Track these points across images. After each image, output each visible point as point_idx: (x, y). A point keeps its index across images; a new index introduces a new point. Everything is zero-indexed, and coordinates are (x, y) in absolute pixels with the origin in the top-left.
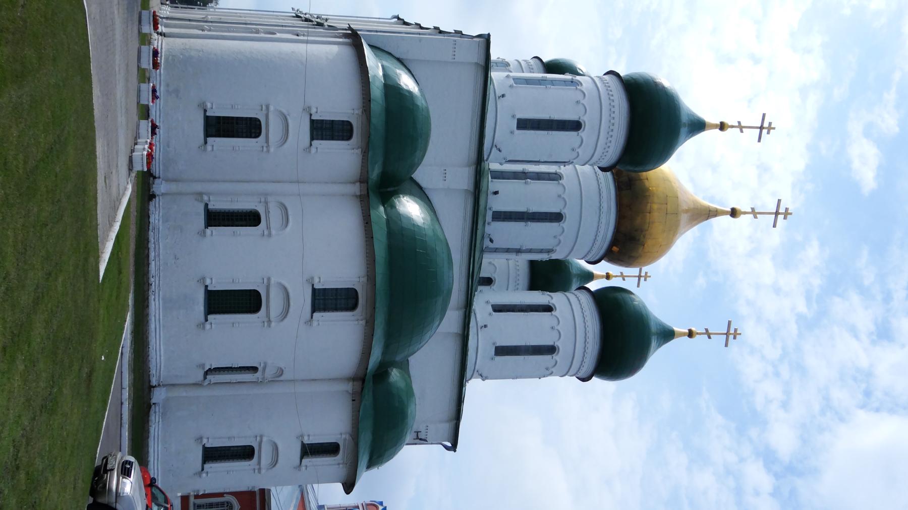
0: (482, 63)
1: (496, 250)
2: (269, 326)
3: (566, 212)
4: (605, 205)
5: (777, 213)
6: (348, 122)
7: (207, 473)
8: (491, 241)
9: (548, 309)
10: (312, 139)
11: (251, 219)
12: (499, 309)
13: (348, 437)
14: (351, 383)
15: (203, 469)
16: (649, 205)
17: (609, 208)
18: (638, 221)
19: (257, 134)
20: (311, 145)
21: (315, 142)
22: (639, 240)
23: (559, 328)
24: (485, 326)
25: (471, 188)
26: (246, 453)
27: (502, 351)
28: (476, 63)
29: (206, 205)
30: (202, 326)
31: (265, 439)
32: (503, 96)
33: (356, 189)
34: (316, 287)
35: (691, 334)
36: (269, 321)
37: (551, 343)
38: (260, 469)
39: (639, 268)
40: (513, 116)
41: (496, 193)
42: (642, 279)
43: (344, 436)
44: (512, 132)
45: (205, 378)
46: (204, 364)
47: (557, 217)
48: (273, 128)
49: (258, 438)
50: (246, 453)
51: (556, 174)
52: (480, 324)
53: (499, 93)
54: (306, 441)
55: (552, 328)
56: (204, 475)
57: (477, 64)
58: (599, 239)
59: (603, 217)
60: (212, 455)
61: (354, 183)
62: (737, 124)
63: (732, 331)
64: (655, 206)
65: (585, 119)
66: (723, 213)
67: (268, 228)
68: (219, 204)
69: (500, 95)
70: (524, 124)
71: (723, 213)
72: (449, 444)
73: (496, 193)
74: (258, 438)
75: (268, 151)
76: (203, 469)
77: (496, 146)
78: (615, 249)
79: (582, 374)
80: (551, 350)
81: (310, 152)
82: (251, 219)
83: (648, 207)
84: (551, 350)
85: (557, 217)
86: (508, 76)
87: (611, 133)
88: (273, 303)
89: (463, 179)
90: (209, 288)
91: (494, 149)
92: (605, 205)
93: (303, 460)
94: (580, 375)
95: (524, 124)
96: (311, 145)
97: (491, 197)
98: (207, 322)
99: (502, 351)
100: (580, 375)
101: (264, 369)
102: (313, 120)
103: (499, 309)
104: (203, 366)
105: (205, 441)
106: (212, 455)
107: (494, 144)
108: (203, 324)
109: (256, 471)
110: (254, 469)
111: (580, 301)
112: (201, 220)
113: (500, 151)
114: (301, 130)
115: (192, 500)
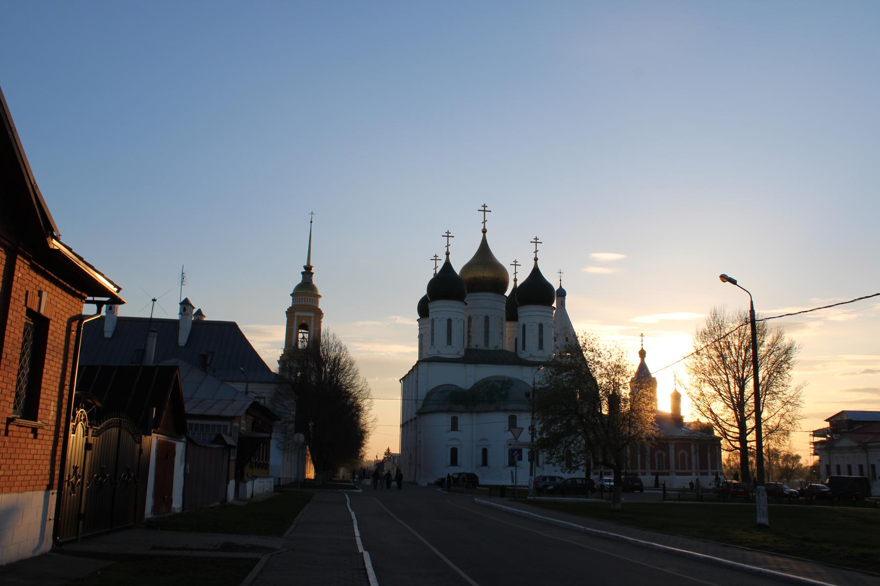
0: (427, 363)
5: (485, 211)
6: (452, 418)
10: (457, 430)
11: (485, 451)
21: (459, 429)
29: (480, 466)
33: (474, 415)
34: (508, 429)
40: (446, 347)
41: (477, 346)
45: (540, 467)
48: (454, 444)
51: (468, 318)
62: (447, 248)
68: (480, 462)
70: (449, 341)
82: (485, 451)
89: (471, 369)
95: (449, 341)
97: (479, 348)
112: (484, 468)
114: (454, 434)
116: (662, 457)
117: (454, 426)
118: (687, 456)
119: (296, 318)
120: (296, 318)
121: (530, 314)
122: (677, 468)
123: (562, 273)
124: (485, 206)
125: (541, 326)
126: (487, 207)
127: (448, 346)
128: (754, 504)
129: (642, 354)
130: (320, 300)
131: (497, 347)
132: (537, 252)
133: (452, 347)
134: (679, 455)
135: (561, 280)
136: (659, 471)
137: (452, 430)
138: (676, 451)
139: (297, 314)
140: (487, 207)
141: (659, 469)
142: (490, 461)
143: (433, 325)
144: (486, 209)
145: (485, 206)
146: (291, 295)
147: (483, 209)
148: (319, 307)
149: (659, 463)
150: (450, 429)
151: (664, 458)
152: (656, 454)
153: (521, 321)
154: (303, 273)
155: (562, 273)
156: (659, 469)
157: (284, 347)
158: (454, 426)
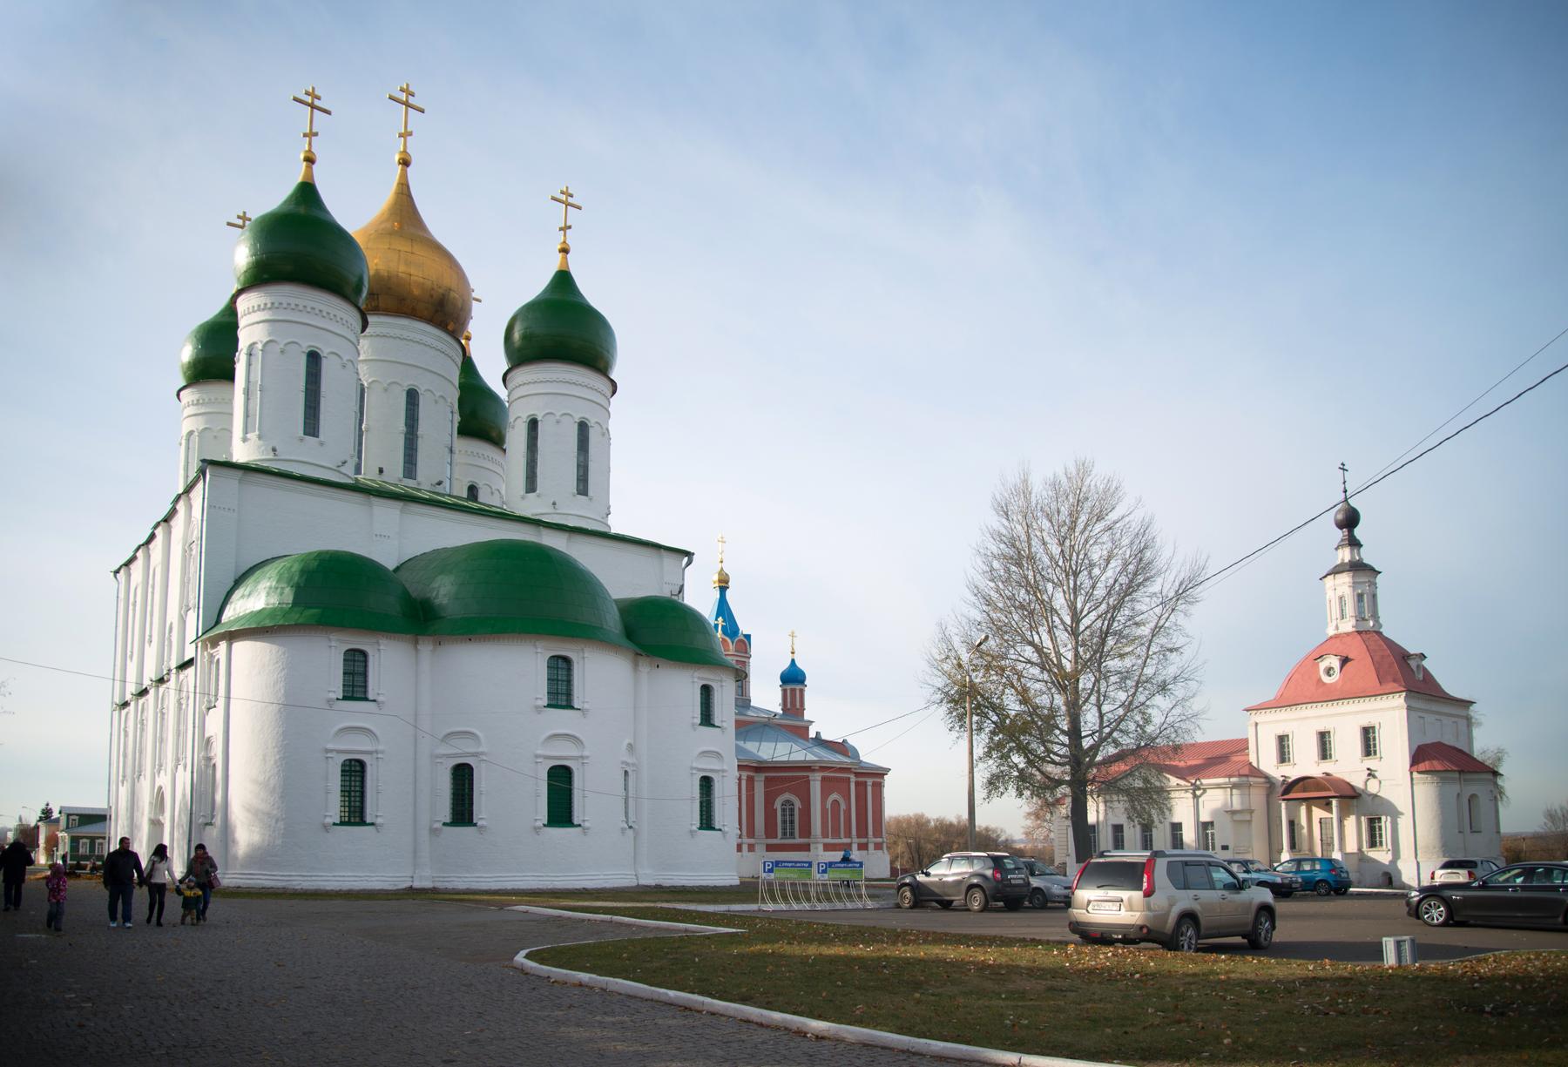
2: (587, 757)
3: (407, 384)
4: (397, 332)
7: (724, 825)
9: (533, 424)
11: (463, 776)
12: (531, 485)
13: (696, 674)
14: (640, 668)
15: (720, 830)
16: (400, 274)
18: (416, 292)
19: (362, 764)
20: (374, 701)
22: (443, 295)
23: (558, 414)
24: (554, 504)
25: (401, 504)
26: (706, 783)
27: (583, 487)
28: (239, 483)
30: (585, 830)
31: (695, 765)
32: (274, 450)
33: (426, 648)
35: (565, 251)
36: (582, 757)
37: (576, 426)
38: (723, 771)
39: (474, 302)
43: (696, 680)
44: (322, 444)
46: (622, 829)
47: (412, 396)
49: (694, 772)
50: (706, 783)
52: (551, 510)
53: (271, 456)
54: (698, 721)
55: (558, 422)
56: (726, 829)
57: (240, 481)
58: (440, 346)
59: (412, 335)
60: (707, 822)
61: (417, 650)
64: (402, 268)
66: (404, 176)
67: (475, 755)
68: (445, 811)
69: (272, 454)
71: (404, 176)
72: (686, 559)
73: (381, 471)
74: (694, 772)
75: (382, 752)
76: (720, 830)
77: (339, 466)
79: (607, 389)
80: (583, 428)
81: (383, 703)
82: (463, 776)
83: (404, 276)
84: (583, 428)
85: (412, 396)
87: (325, 314)
88: (563, 753)
89: (386, 513)
90: (546, 823)
91: (343, 469)
92: (397, 332)
93: (716, 724)
94: (609, 394)
96: (374, 701)
97: (385, 477)
98: (582, 824)
99: (583, 487)
100: (608, 392)
101: (627, 764)
102: (344, 697)
103: (531, 485)
104: (623, 830)
105: (694, 828)
106: (707, 822)
107: (335, 468)
108: (584, 829)
109: (725, 774)
110: (723, 776)
111: (525, 384)
113: (344, 463)
116: (792, 810)
117: (356, 685)
118: (843, 807)
122: (825, 835)
127: (308, 438)
131: (440, 483)
133: (322, 444)
137: (345, 698)
138: (825, 796)
142: (482, 808)
150: (341, 698)
152: (778, 805)
158: (356, 685)
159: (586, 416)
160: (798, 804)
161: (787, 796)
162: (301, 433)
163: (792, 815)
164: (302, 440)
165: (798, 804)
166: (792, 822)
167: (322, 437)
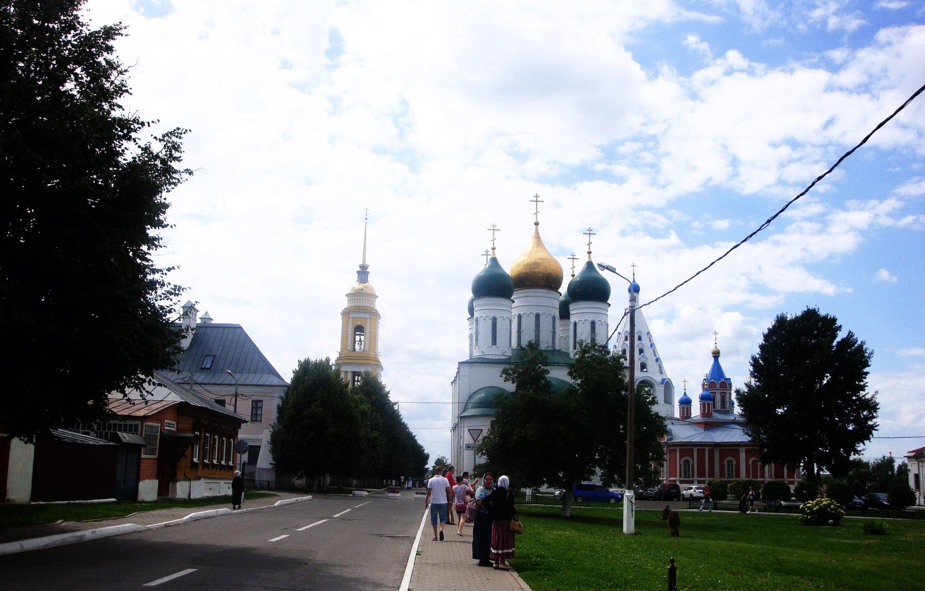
1: (554, 343)
3: (535, 313)
4: (532, 294)
8: (548, 347)
9: (575, 324)
17: (533, 292)
23: (583, 320)
32: (483, 352)
42: (574, 257)
47: (538, 316)
51: (518, 317)
53: (482, 354)
57: (470, 366)
63: (588, 232)
65: (491, 316)
66: (537, 229)
70: (494, 342)
71: (537, 229)
78: (553, 286)
85: (538, 316)
86: (475, 349)
92: (532, 294)
95: (494, 342)
115: (681, 479)
116: (732, 465)
119: (351, 319)
120: (351, 319)
121: (580, 312)
123: (636, 266)
124: (537, 196)
125: (593, 323)
126: (539, 197)
127: (493, 346)
128: (621, 508)
129: (716, 355)
130: (377, 300)
132: (591, 245)
134: (750, 462)
135: (634, 275)
136: (729, 479)
139: (351, 316)
140: (539, 197)
141: (729, 477)
143: (477, 324)
144: (539, 199)
145: (537, 196)
146: (347, 295)
147: (535, 200)
148: (376, 308)
149: (729, 470)
151: (734, 466)
152: (725, 462)
153: (573, 319)
154: (358, 272)
155: (636, 266)
156: (729, 477)
157: (339, 350)
159: (594, 319)
160: (734, 462)
161: (729, 458)
162: (491, 345)
163: (732, 467)
164: (491, 347)
165: (734, 462)
166: (732, 470)
167: (497, 345)
